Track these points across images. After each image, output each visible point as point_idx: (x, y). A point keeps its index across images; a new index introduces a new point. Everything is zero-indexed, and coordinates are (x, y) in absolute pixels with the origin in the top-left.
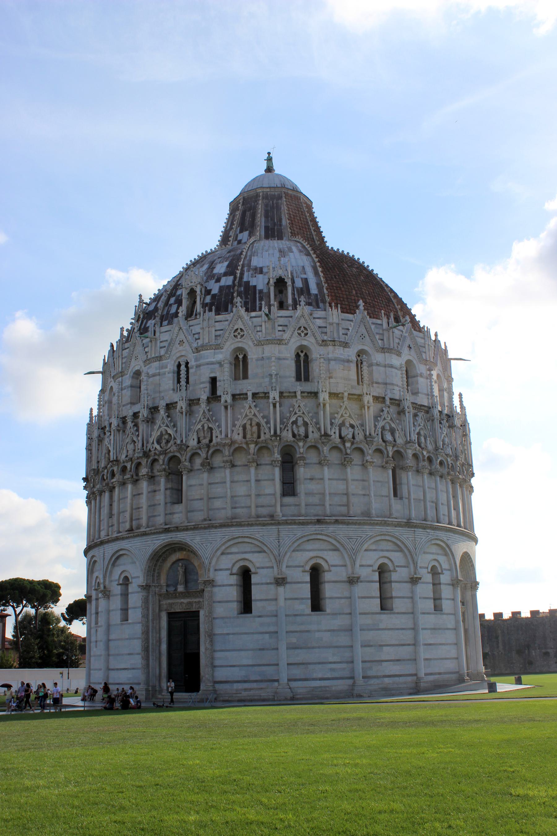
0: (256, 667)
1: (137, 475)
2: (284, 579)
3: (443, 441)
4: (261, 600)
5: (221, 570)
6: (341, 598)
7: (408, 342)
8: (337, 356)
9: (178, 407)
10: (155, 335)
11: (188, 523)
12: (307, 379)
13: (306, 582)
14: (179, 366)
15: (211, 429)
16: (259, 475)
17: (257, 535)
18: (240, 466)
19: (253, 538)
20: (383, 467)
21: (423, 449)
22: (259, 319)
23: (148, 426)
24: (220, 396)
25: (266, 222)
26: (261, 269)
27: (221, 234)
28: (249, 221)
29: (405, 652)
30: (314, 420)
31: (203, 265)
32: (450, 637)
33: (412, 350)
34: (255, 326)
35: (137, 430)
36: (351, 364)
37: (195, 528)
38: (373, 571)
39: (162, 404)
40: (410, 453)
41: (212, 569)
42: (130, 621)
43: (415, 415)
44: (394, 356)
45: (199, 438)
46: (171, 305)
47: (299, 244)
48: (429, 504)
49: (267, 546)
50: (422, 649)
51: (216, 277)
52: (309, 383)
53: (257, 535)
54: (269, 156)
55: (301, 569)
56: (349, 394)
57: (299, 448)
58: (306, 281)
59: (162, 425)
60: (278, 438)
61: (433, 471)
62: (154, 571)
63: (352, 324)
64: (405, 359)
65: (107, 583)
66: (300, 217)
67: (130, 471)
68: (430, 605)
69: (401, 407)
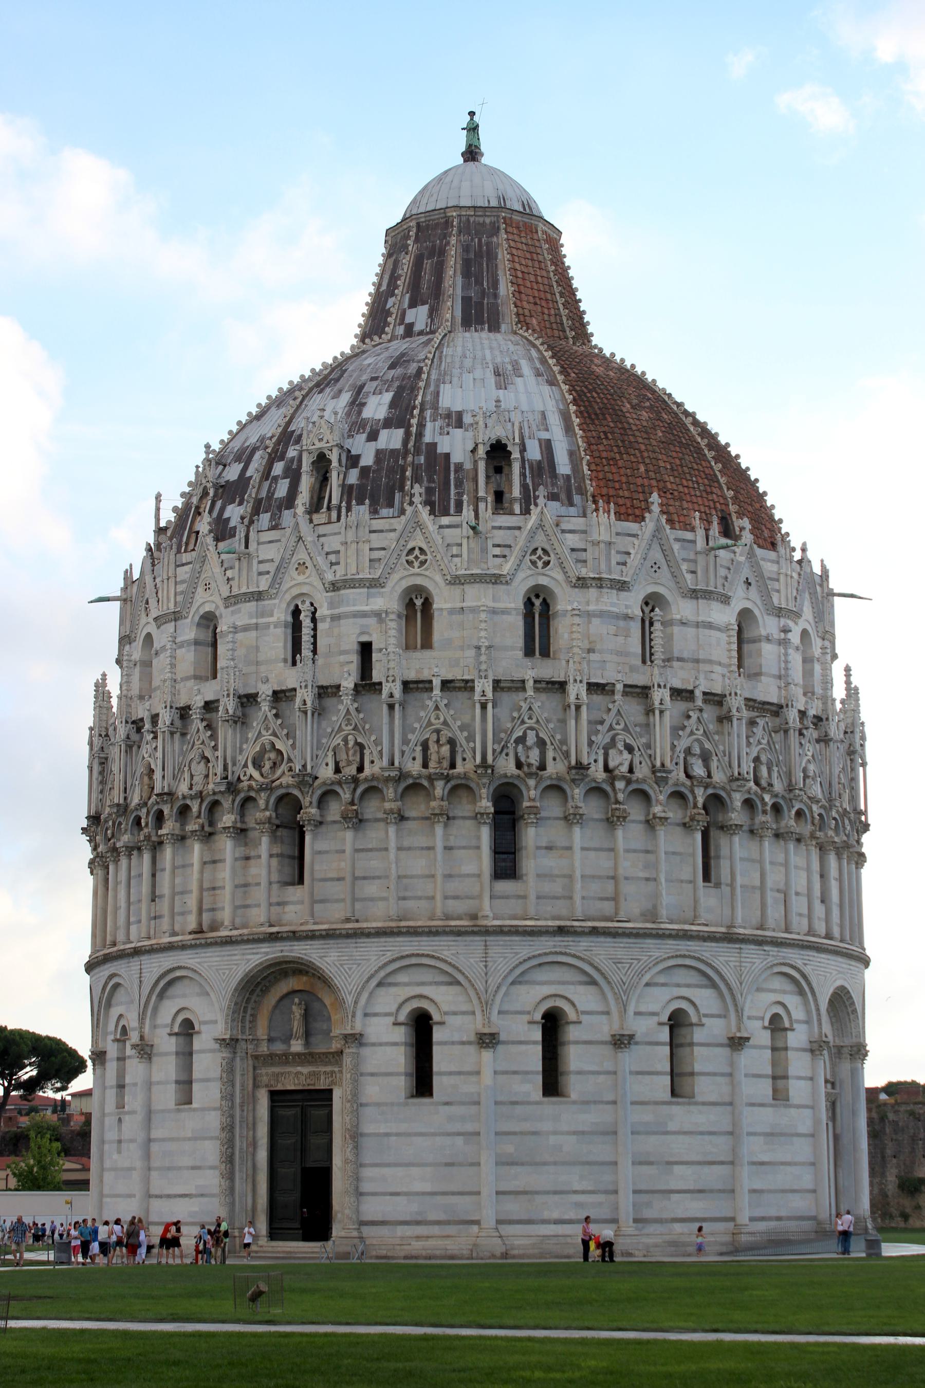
0: (439, 1198)
1: (211, 824)
2: (493, 1036)
3: (805, 770)
4: (450, 1073)
5: (376, 1015)
6: (598, 1073)
7: (746, 572)
8: (605, 608)
9: (298, 700)
10: (247, 547)
11: (314, 924)
12: (546, 653)
13: (535, 1043)
14: (296, 612)
15: (361, 747)
16: (452, 838)
17: (445, 953)
18: (414, 819)
19: (438, 958)
20: (684, 824)
21: (763, 789)
22: (457, 531)
23: (235, 730)
24: (380, 684)
25: (464, 288)
26: (460, 415)
27: (369, 299)
28: (429, 280)
29: (713, 1176)
30: (558, 737)
31: (340, 391)
32: (802, 1150)
33: (753, 588)
34: (448, 545)
35: (213, 737)
36: (632, 623)
37: (329, 935)
38: (660, 1024)
39: (265, 691)
40: (737, 799)
41: (359, 1014)
42: (194, 1105)
43: (752, 723)
44: (715, 605)
45: (337, 764)
46: (276, 479)
47: (534, 353)
48: (770, 896)
49: (463, 974)
50: (745, 1172)
51: (368, 429)
52: (548, 662)
53: (445, 953)
54: (472, 119)
55: (526, 1018)
56: (625, 686)
57: (529, 789)
58: (547, 447)
59: (264, 732)
60: (489, 771)
61: (782, 831)
62: (245, 1011)
63: (636, 542)
64: (738, 609)
65: (147, 1029)
66: (536, 275)
67: (199, 817)
68: (764, 1089)
69: (725, 708)
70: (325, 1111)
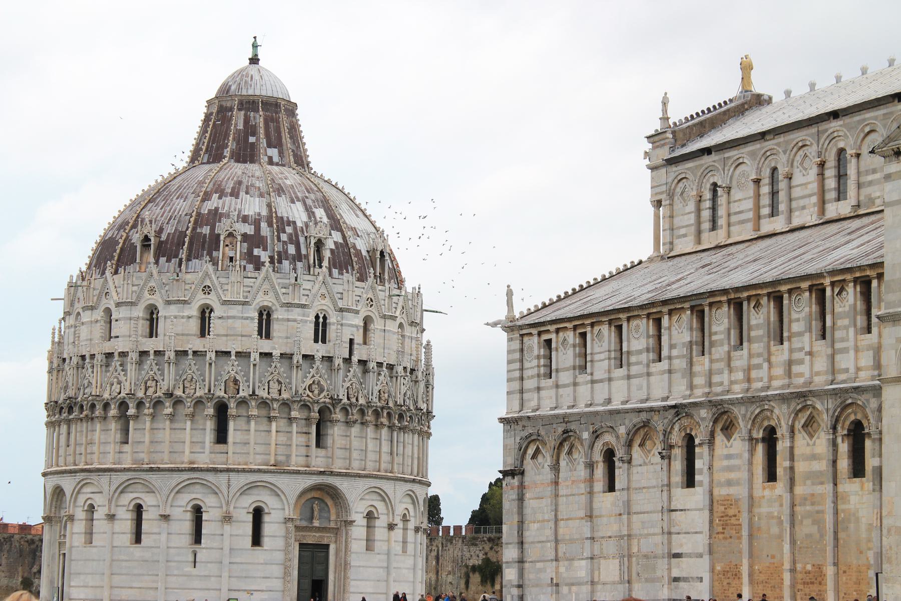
14: (317, 317)
37: (347, 475)
42: (265, 548)
46: (284, 242)
65: (231, 508)
70: (323, 554)
